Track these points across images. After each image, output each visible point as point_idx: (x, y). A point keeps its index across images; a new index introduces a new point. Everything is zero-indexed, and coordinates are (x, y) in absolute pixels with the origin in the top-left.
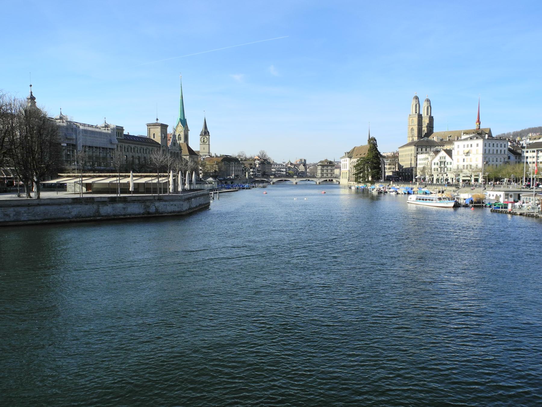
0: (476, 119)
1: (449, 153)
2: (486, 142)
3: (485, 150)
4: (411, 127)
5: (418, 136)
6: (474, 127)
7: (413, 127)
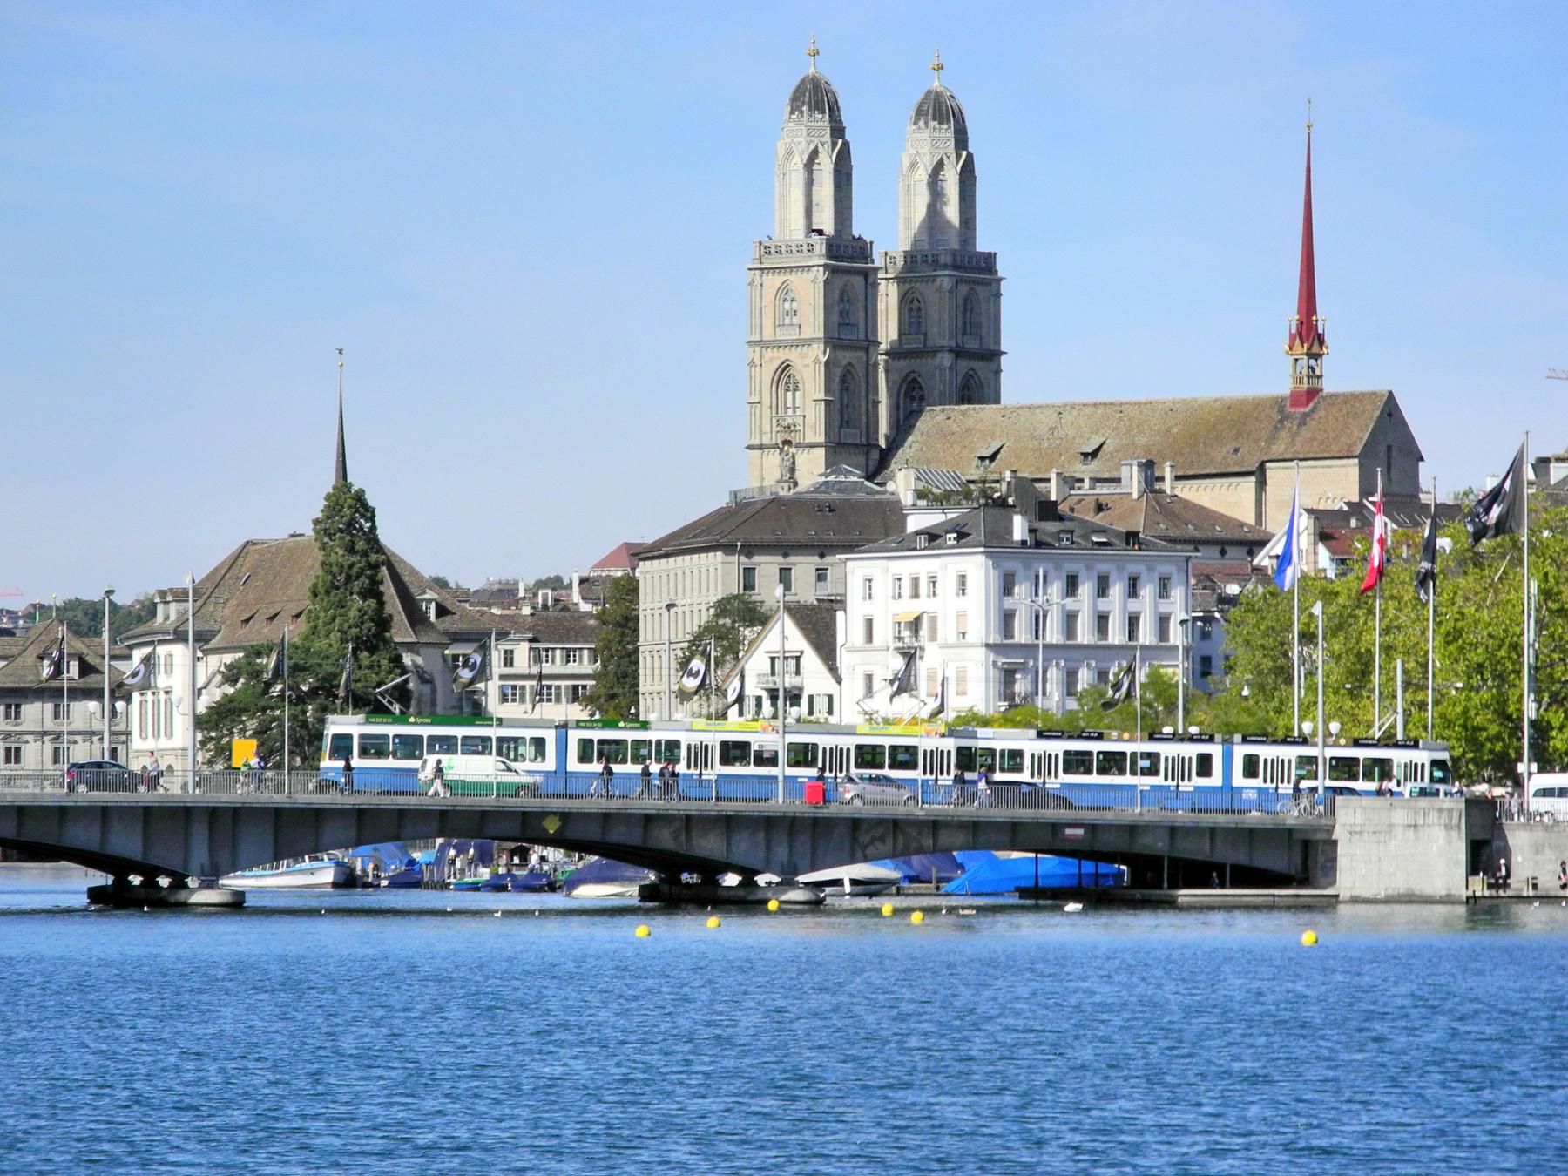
0: (1290, 314)
4: (775, 357)
6: (1275, 376)
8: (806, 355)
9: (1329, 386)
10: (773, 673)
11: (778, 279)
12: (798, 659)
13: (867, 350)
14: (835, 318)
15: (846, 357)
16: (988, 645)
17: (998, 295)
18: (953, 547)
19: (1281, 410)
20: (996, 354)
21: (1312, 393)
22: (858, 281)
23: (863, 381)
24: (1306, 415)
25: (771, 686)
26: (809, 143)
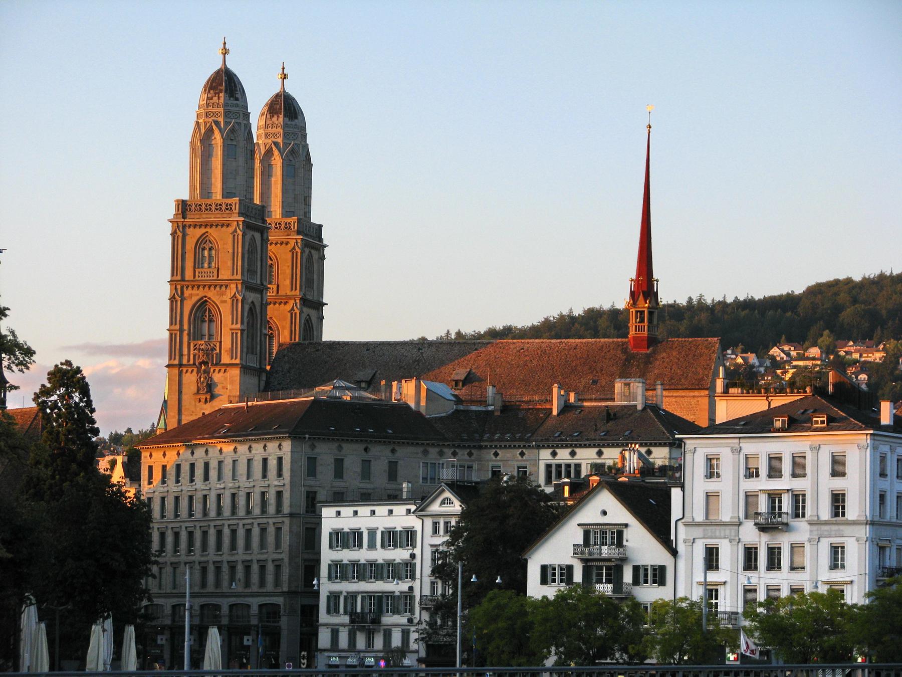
1: (650, 501)
2: (885, 448)
3: (882, 497)
4: (193, 296)
5: (245, 369)
7: (212, 294)
8: (223, 294)
11: (199, 232)
12: (620, 534)
13: (261, 292)
14: (246, 266)
15: (252, 297)
16: (872, 523)
17: (323, 258)
18: (822, 430)
19: (625, 351)
20: (319, 305)
22: (257, 236)
23: (259, 316)
24: (648, 356)
25: (586, 556)
26: (227, 123)
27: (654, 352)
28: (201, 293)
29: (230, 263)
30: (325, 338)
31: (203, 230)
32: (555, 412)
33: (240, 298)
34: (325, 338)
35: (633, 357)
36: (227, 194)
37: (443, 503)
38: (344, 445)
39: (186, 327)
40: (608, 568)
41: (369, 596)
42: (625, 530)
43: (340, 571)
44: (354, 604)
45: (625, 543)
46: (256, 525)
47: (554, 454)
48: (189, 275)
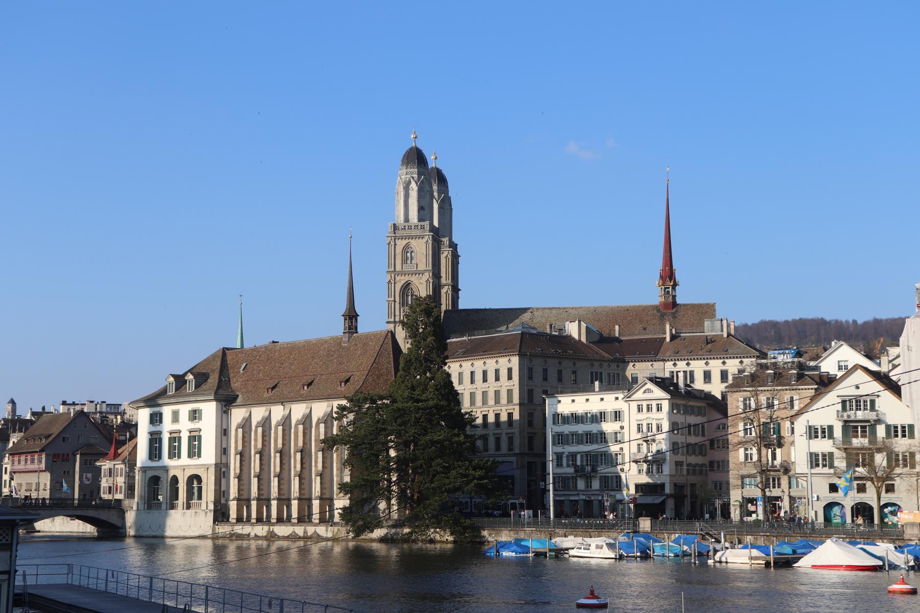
4: (401, 280)
7: (414, 279)
8: (421, 279)
9: (679, 301)
10: (844, 409)
11: (404, 242)
12: (873, 403)
19: (658, 311)
21: (675, 304)
24: (674, 314)
25: (845, 418)
27: (677, 311)
28: (407, 278)
29: (424, 261)
30: (460, 308)
31: (407, 241)
32: (668, 339)
33: (431, 281)
34: (460, 308)
35: (665, 314)
36: (420, 219)
37: (645, 392)
38: (548, 360)
39: (397, 299)
40: (862, 427)
41: (587, 454)
42: (877, 400)
43: (560, 439)
44: (574, 460)
45: (877, 408)
46: (491, 411)
47: (675, 365)
48: (398, 268)
